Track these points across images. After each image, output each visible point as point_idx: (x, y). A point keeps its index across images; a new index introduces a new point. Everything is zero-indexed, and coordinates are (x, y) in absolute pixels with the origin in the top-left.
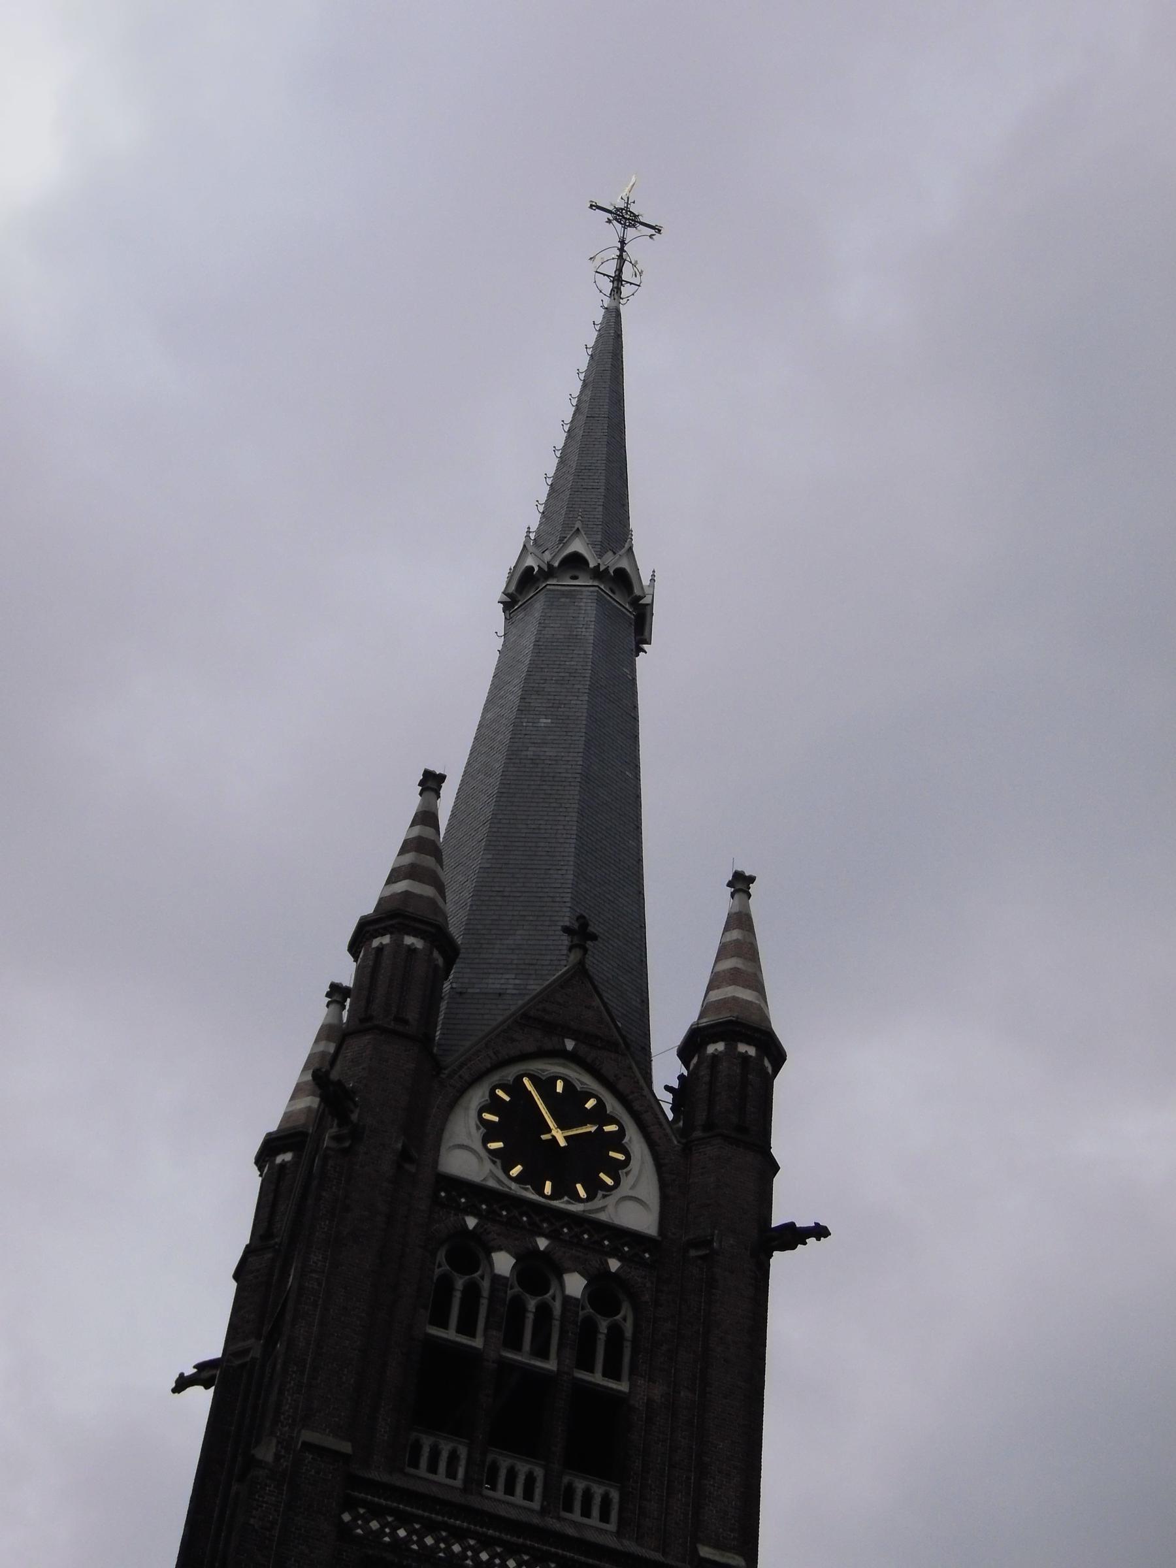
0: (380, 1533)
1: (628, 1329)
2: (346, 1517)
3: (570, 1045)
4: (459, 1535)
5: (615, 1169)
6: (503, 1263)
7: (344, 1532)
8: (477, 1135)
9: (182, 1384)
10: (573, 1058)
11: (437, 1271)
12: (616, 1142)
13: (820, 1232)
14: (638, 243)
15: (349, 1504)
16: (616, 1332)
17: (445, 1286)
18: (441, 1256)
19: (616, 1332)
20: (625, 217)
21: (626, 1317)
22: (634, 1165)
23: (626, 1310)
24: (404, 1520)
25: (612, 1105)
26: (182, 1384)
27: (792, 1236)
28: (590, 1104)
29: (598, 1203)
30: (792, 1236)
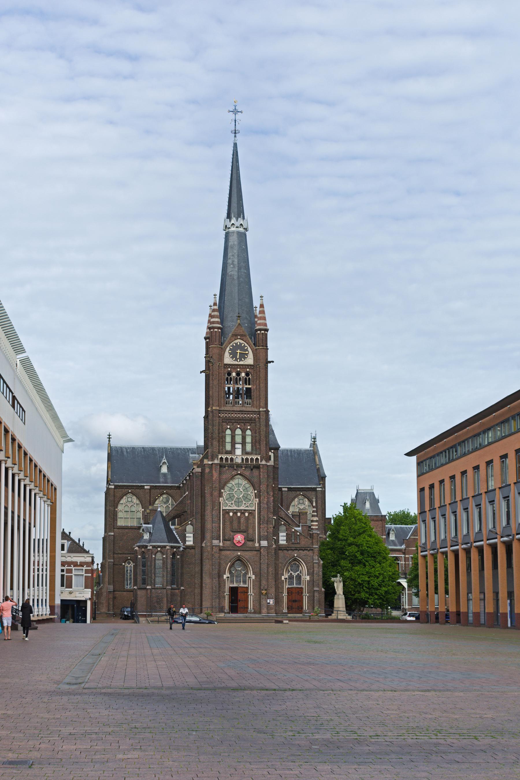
0: (224, 416)
1: (251, 378)
3: (239, 337)
4: (232, 413)
6: (234, 374)
7: (219, 417)
8: (229, 355)
9: (201, 372)
10: (240, 339)
11: (226, 377)
13: (273, 362)
15: (219, 413)
16: (249, 378)
17: (227, 378)
18: (226, 375)
19: (249, 378)
20: (235, 112)
21: (250, 376)
22: (249, 354)
23: (250, 375)
24: (226, 413)
26: (201, 372)
27: (270, 362)
28: (243, 345)
30: (270, 362)
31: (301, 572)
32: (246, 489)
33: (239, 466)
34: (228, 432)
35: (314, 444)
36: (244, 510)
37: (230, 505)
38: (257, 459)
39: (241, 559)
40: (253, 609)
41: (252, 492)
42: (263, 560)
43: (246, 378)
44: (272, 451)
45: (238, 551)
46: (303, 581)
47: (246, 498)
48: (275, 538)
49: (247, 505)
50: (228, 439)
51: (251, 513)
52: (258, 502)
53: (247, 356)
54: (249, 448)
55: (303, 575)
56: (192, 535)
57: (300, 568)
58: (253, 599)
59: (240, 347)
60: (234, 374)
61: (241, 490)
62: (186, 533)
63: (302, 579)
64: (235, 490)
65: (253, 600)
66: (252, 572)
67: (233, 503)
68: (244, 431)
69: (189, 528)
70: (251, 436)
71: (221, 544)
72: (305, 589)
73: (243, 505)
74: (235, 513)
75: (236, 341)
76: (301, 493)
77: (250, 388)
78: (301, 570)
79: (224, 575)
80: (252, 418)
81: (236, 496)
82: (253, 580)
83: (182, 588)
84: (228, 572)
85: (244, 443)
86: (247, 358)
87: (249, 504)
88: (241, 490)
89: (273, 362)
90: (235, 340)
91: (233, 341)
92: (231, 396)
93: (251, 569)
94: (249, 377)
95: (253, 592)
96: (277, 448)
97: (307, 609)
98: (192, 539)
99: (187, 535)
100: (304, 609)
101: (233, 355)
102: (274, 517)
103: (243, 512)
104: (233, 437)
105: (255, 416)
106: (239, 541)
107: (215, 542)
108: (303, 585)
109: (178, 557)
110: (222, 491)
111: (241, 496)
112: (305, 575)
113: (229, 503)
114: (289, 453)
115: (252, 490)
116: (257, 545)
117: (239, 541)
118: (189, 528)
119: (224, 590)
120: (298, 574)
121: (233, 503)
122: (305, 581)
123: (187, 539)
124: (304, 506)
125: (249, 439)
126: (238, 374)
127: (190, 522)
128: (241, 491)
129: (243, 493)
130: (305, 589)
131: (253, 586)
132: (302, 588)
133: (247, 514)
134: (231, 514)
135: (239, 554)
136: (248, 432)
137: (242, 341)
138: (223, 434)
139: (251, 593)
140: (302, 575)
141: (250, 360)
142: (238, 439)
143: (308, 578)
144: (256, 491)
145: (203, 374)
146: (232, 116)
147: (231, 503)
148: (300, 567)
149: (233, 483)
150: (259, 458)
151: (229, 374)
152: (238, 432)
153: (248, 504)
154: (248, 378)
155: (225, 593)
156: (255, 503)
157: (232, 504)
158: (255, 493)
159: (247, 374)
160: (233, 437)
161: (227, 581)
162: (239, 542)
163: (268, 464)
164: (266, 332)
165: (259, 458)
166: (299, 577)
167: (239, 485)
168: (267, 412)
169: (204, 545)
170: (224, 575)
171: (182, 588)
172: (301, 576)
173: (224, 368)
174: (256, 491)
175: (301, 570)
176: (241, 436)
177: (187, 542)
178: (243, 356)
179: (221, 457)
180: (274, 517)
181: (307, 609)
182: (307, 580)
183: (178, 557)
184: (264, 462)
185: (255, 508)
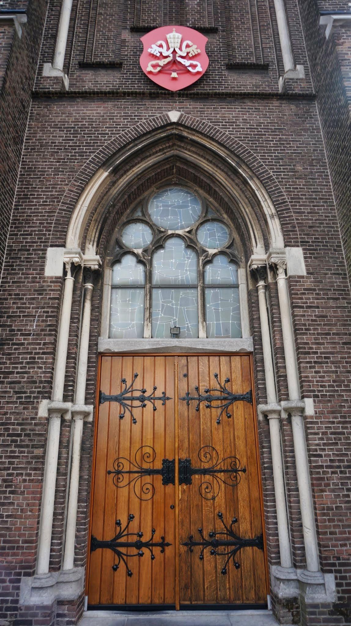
39: (188, 155)
40: (325, 567)
45: (157, 104)
58: (311, 454)
65: (312, 470)
66: (275, 226)
79: (51, 251)
82: (291, 281)
84: (93, 234)
93: (268, 208)
95: (302, 381)
106: (174, 62)
117: (174, 62)
119: (38, 373)
131: (296, 331)
135: (174, 116)
155: (49, 396)
161: (77, 304)
170: (51, 251)
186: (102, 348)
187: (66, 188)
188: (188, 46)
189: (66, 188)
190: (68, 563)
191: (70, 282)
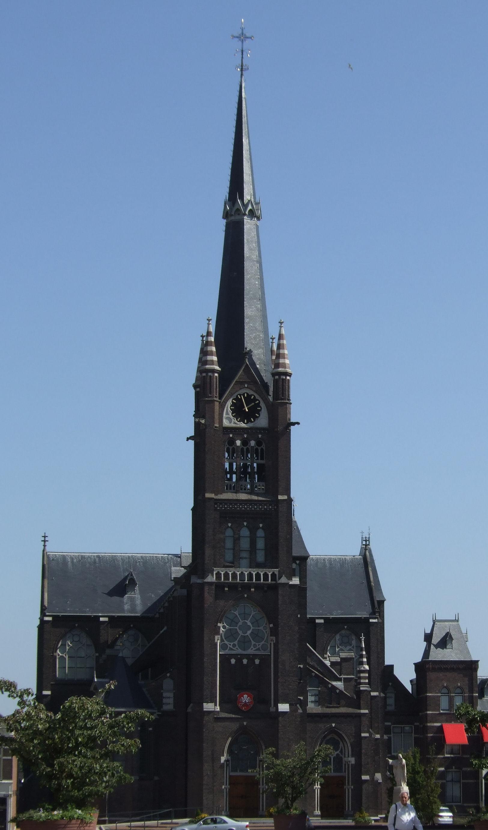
1: (264, 448)
2: (216, 506)
5: (259, 412)
6: (238, 443)
9: (188, 439)
12: (258, 405)
13: (298, 423)
14: (247, 42)
15: (216, 504)
16: (262, 449)
18: (226, 444)
19: (262, 449)
20: (242, 37)
21: (263, 446)
22: (263, 410)
23: (264, 444)
25: (257, 397)
26: (188, 439)
27: (294, 424)
28: (252, 397)
29: (256, 421)
30: (294, 424)
31: (341, 752)
32: (255, 622)
33: (246, 587)
34: (229, 532)
35: (366, 548)
36: (254, 655)
37: (231, 647)
38: (273, 575)
41: (265, 628)
42: (282, 733)
43: (257, 449)
44: (298, 562)
46: (345, 764)
47: (256, 635)
48: (302, 698)
49: (258, 647)
50: (229, 544)
51: (265, 659)
52: (274, 642)
53: (259, 415)
54: (260, 557)
55: (345, 757)
56: (171, 695)
57: (341, 745)
59: (249, 399)
60: (238, 443)
61: (249, 624)
62: (162, 691)
63: (344, 763)
64: (240, 624)
67: (237, 644)
68: (253, 531)
69: (168, 684)
70: (263, 539)
71: (218, 708)
72: (349, 778)
73: (252, 647)
74: (239, 658)
75: (242, 391)
76: (346, 627)
77: (263, 465)
78: (342, 749)
79: (221, 757)
80: (266, 509)
81: (240, 632)
83: (156, 778)
85: (253, 549)
86: (260, 418)
87: (260, 646)
88: (249, 624)
89: (298, 423)
90: (241, 389)
91: (237, 391)
92: (234, 476)
94: (262, 447)
96: (304, 559)
97: (350, 809)
98: (171, 701)
99: (165, 695)
100: (347, 810)
101: (238, 411)
102: (299, 666)
103: (251, 658)
104: (237, 540)
105: (270, 507)
107: (208, 707)
108: (345, 772)
109: (151, 729)
110: (219, 624)
111: (249, 632)
112: (348, 757)
113: (230, 645)
114: (328, 565)
115: (266, 624)
116: (272, 709)
118: (168, 684)
120: (337, 754)
121: (237, 644)
122: (348, 765)
123: (165, 701)
124: (350, 647)
125: (261, 544)
126: (245, 442)
127: (168, 675)
128: (249, 626)
129: (252, 628)
130: (349, 778)
132: (344, 777)
133: (257, 661)
134: (233, 661)
136: (260, 533)
137: (251, 392)
138: (222, 536)
139: (263, 784)
140: (343, 756)
141: (262, 421)
142: (245, 544)
143: (352, 760)
144: (271, 625)
145: (192, 442)
146: (237, 44)
147: (232, 643)
148: (341, 743)
149: (236, 613)
150: (277, 573)
151: (232, 442)
152: (245, 532)
153: (259, 645)
154: (259, 448)
156: (271, 644)
157: (234, 645)
158: (271, 628)
159: (259, 443)
160: (237, 540)
162: (245, 704)
163: (291, 583)
164: (288, 378)
165: (277, 573)
166: (338, 760)
167: (245, 616)
168: (290, 501)
169: (189, 710)
170: (221, 757)
171: (156, 778)
172: (342, 758)
173: (224, 434)
174: (271, 625)
175: (342, 749)
176: (249, 539)
177: (164, 706)
178: (253, 414)
179: (218, 572)
180: (299, 666)
181: (350, 809)
182: (352, 764)
183: (151, 729)
184: (283, 580)
185: (271, 653)
186: (230, 775)
187: (223, 743)
188: (249, 699)
189: (223, 743)
190: (228, 810)
191: (225, 763)
